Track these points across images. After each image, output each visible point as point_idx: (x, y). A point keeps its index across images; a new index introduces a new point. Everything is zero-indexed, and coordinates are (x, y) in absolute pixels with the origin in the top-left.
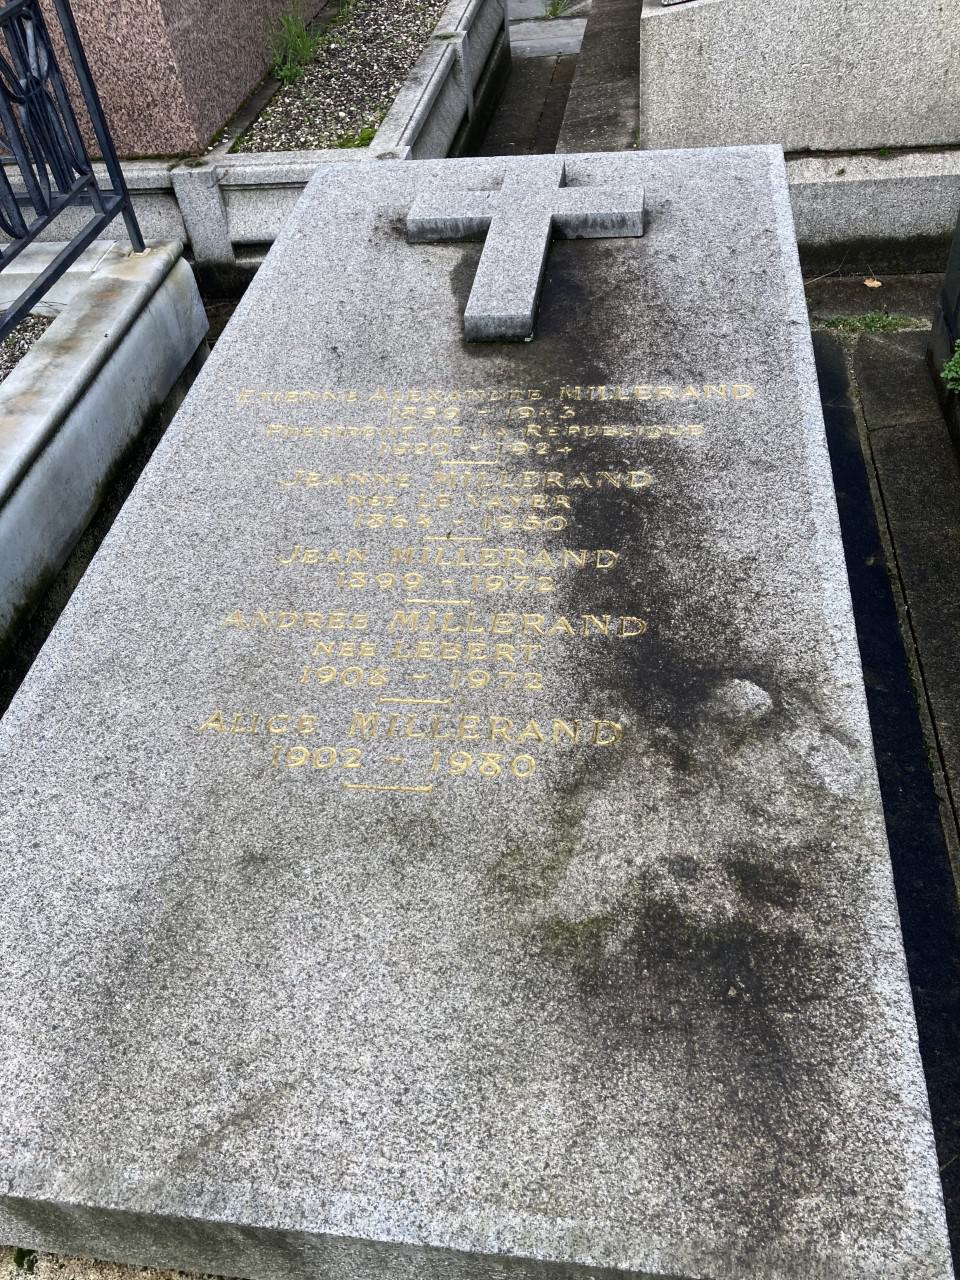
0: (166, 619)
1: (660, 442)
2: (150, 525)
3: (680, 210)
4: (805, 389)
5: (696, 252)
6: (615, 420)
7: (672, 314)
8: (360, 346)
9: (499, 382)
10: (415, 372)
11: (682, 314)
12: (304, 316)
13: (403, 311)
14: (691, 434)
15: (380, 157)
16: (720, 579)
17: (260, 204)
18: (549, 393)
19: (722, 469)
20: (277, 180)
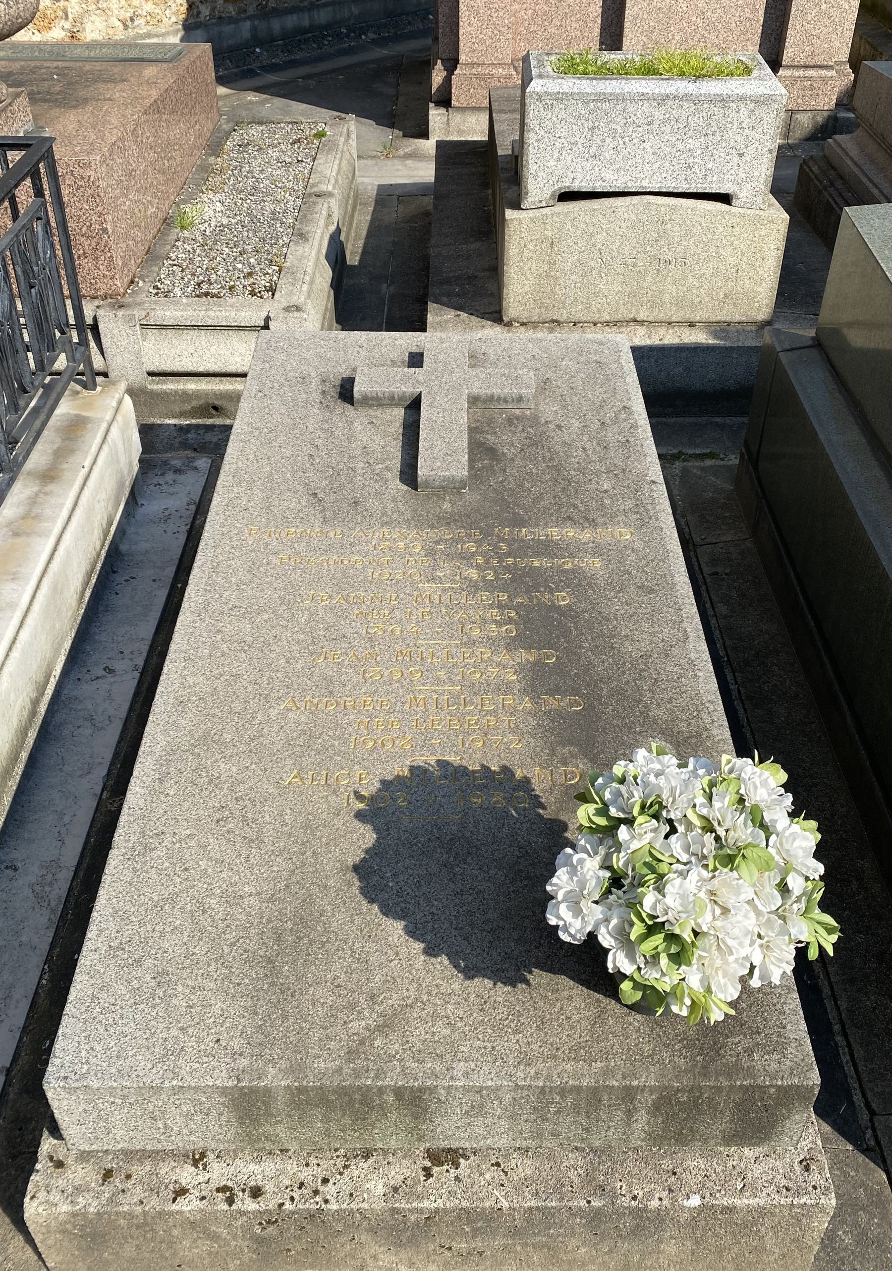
0: (238, 706)
1: (573, 571)
2: (205, 634)
3: (559, 387)
4: (668, 533)
5: (576, 424)
6: (538, 555)
7: (566, 473)
8: (335, 493)
9: (448, 523)
10: (383, 515)
11: (572, 473)
12: (284, 466)
13: (362, 465)
14: (594, 565)
15: (287, 309)
16: (629, 670)
17: (174, 341)
18: (487, 533)
19: (619, 592)
20: (193, 323)
